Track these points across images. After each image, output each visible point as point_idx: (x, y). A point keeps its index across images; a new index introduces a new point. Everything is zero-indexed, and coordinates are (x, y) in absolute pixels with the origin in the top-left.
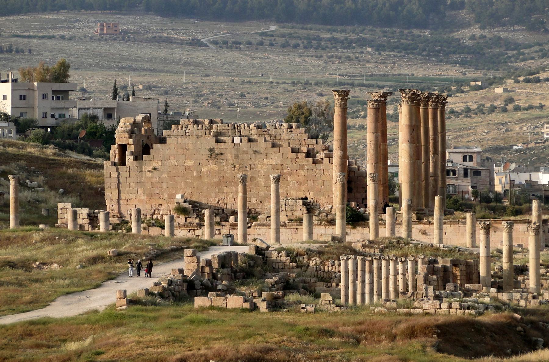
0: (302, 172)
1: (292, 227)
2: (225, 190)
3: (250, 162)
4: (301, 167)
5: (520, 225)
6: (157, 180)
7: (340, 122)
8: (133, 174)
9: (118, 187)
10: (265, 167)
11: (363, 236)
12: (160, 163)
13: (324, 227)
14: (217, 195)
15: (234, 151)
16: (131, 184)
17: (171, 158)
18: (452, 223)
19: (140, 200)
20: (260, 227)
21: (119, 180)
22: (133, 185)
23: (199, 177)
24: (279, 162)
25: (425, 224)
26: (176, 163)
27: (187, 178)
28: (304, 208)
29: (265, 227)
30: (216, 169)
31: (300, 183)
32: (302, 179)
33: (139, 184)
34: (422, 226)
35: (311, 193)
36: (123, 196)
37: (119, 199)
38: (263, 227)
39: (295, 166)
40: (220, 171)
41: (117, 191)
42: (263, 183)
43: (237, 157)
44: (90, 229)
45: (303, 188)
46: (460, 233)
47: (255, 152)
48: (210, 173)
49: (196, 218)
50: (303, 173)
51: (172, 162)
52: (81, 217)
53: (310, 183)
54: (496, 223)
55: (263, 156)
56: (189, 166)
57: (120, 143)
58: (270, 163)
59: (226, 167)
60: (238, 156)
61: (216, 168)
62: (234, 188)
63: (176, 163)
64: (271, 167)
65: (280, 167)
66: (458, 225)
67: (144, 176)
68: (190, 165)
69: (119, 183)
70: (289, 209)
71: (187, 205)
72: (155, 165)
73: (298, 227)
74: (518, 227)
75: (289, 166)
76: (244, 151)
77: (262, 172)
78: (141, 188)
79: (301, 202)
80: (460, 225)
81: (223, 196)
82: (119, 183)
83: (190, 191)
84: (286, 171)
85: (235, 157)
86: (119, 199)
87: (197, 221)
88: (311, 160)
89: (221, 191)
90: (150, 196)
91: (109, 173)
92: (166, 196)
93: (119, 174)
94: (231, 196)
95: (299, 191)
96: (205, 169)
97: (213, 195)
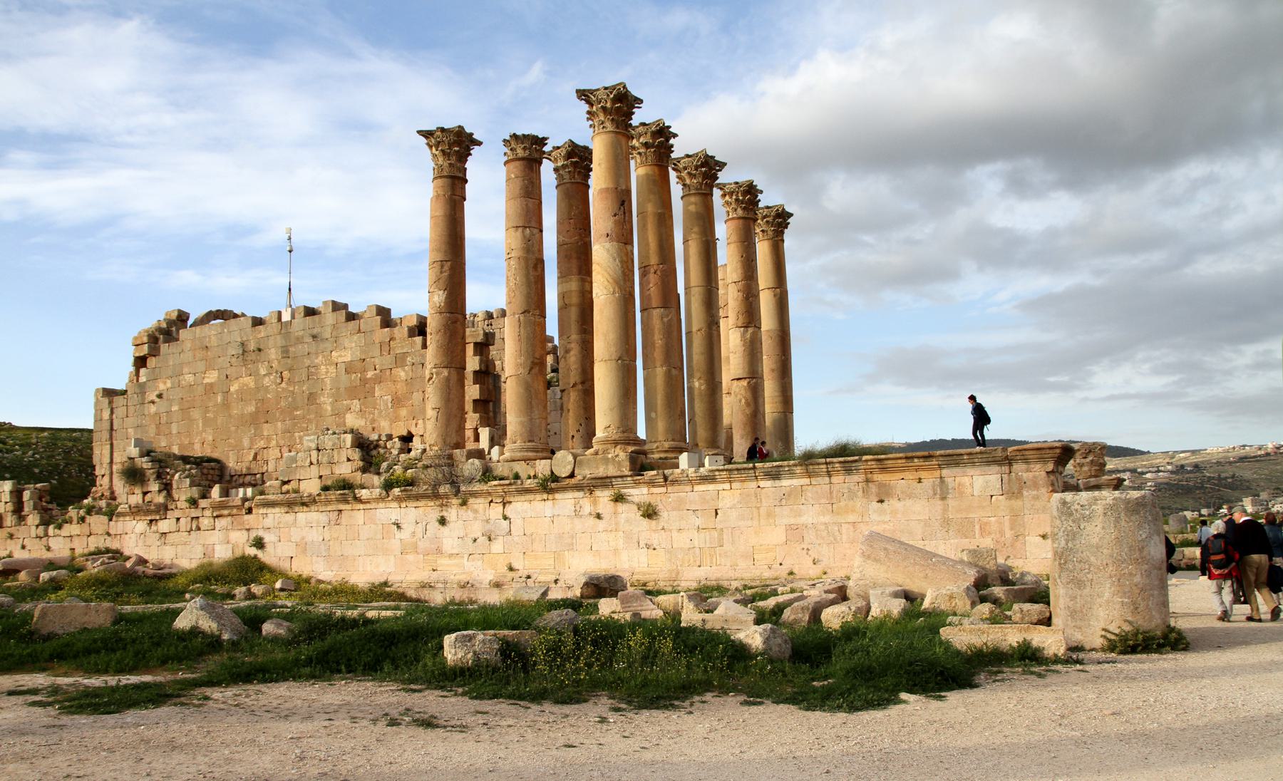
0: (402, 374)
1: (329, 508)
2: (267, 429)
3: (307, 362)
4: (400, 360)
5: (970, 471)
6: (164, 420)
7: (440, 212)
8: (131, 409)
9: (111, 438)
10: (332, 369)
11: (488, 527)
12: (169, 385)
13: (395, 504)
14: (252, 441)
15: (280, 341)
17: (186, 370)
18: (735, 475)
20: (270, 510)
23: (226, 405)
24: (358, 355)
25: (651, 483)
26: (189, 378)
27: (206, 410)
28: (356, 454)
29: (277, 510)
30: (252, 385)
31: (397, 401)
32: (401, 388)
34: (645, 490)
35: (420, 422)
37: (111, 462)
38: (273, 510)
39: (388, 360)
40: (258, 389)
42: (329, 408)
43: (285, 352)
45: (403, 412)
46: (763, 511)
47: (314, 337)
48: (243, 396)
49: (160, 491)
50: (403, 374)
53: (417, 396)
54: (884, 470)
55: (328, 345)
56: (211, 385)
58: (340, 360)
59: (267, 379)
60: (287, 351)
61: (250, 381)
64: (343, 366)
65: (359, 365)
66: (753, 484)
70: (325, 460)
71: (144, 463)
72: (162, 387)
73: (341, 507)
74: (966, 480)
75: (377, 360)
76: (298, 339)
77: (328, 381)
79: (349, 438)
80: (762, 484)
81: (262, 444)
82: (112, 429)
83: (211, 438)
84: (370, 374)
86: (111, 462)
87: (160, 499)
88: (419, 339)
89: (258, 435)
94: (274, 442)
95: (396, 419)
97: (246, 443)
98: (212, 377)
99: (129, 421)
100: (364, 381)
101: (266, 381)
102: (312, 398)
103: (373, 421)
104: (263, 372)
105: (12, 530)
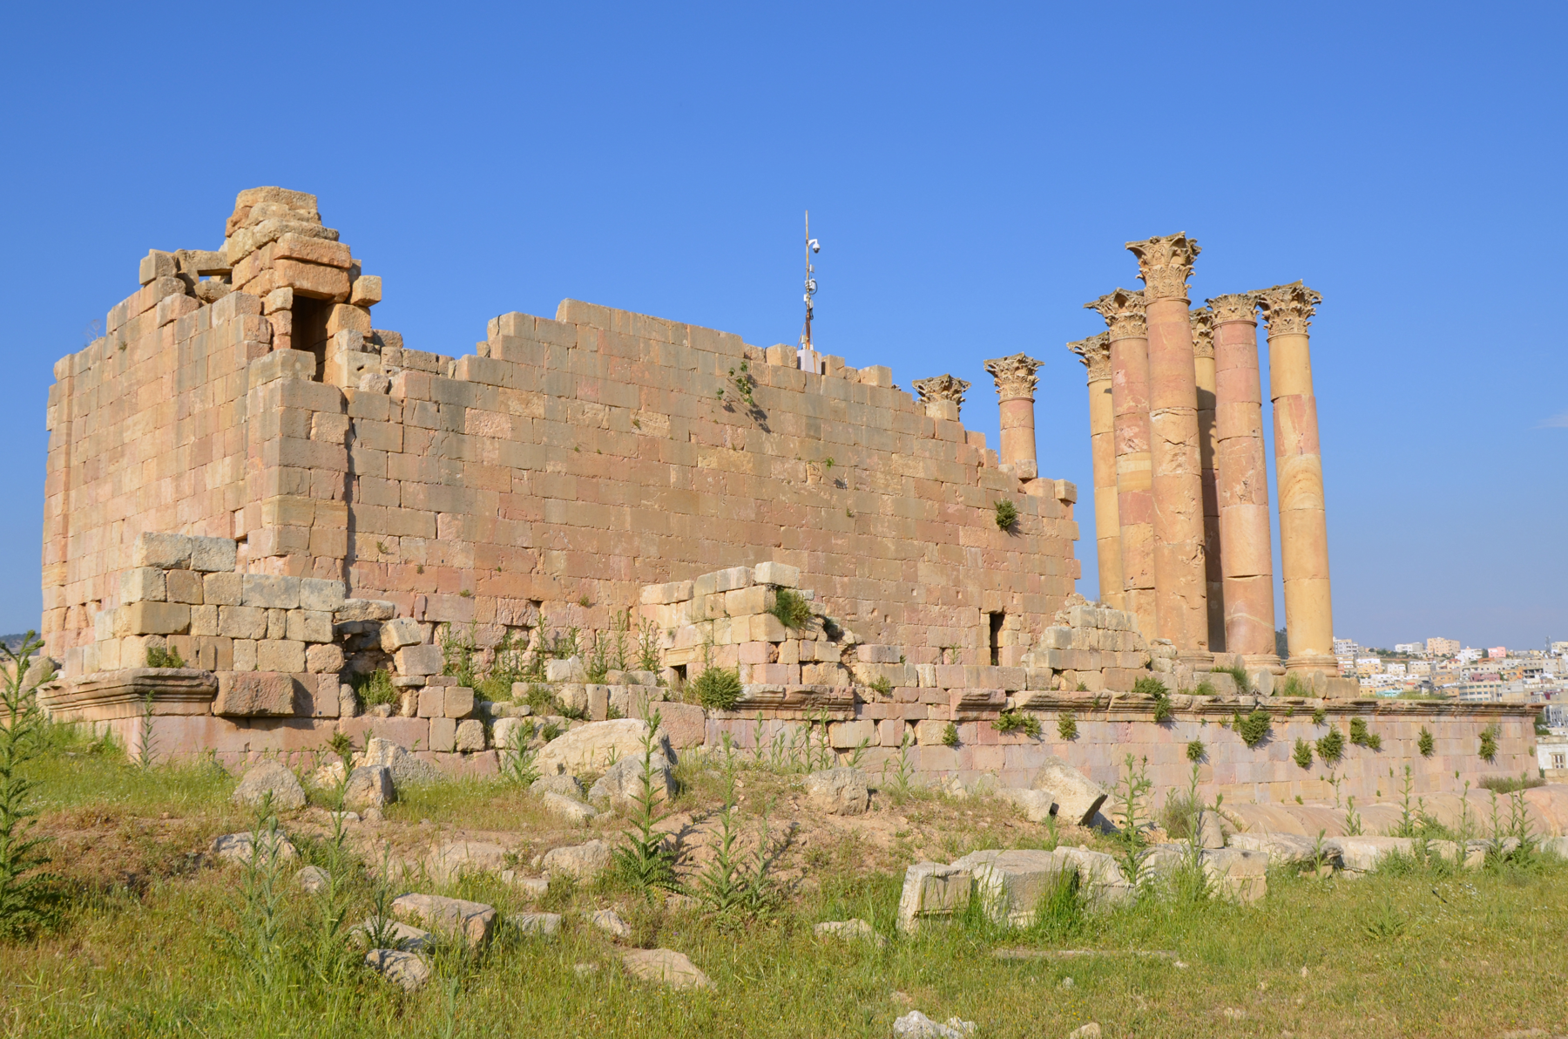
1: (1120, 717)
8: (416, 438)
9: (347, 496)
12: (538, 408)
16: (411, 488)
19: (448, 575)
21: (350, 460)
22: (415, 492)
23: (688, 498)
26: (603, 415)
30: (747, 467)
33: (451, 492)
36: (366, 547)
37: (348, 560)
41: (344, 515)
43: (813, 429)
44: (348, 706)
45: (998, 578)
51: (587, 407)
52: (298, 632)
56: (652, 441)
57: (306, 284)
60: (818, 429)
61: (744, 460)
62: (805, 554)
63: (603, 415)
67: (467, 455)
68: (657, 434)
69: (350, 476)
78: (454, 512)
82: (350, 476)
83: (653, 551)
85: (809, 426)
90: (494, 557)
91: (303, 414)
92: (559, 561)
93: (351, 432)
96: (708, 462)
98: (657, 425)
99: (411, 464)
100: (945, 518)
101: (777, 469)
102: (859, 519)
103: (957, 582)
104: (769, 450)
105: (346, 725)
